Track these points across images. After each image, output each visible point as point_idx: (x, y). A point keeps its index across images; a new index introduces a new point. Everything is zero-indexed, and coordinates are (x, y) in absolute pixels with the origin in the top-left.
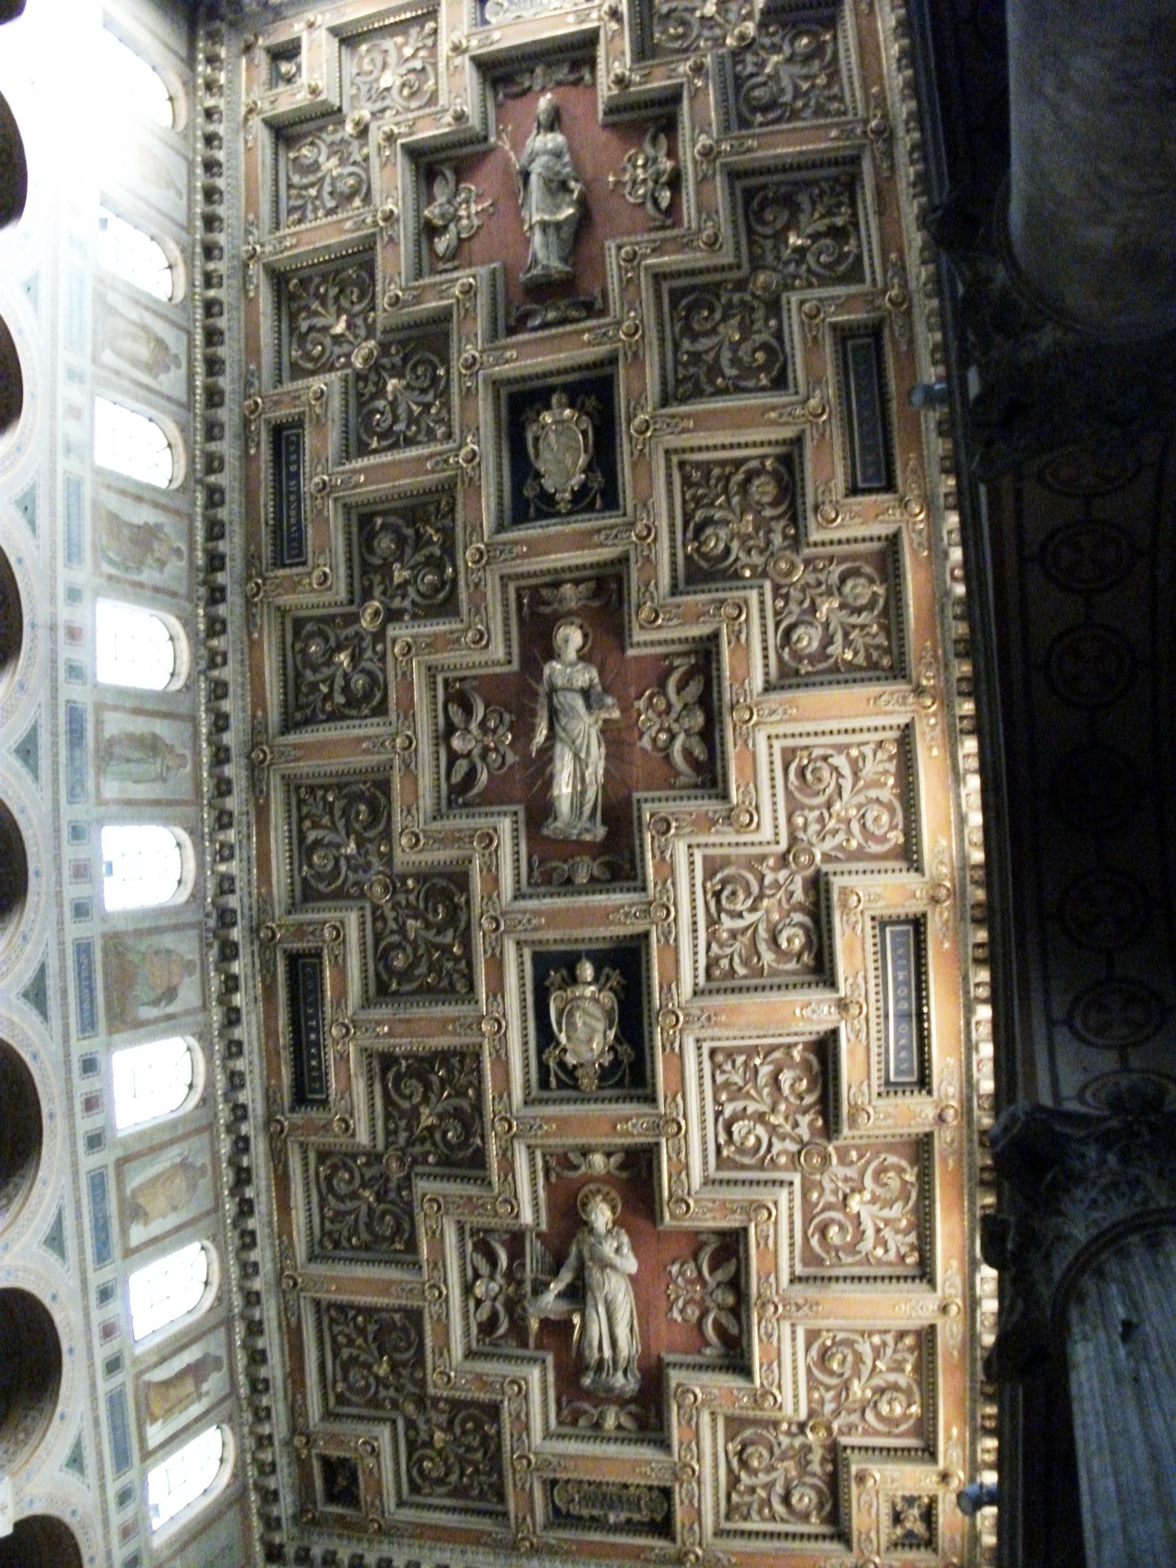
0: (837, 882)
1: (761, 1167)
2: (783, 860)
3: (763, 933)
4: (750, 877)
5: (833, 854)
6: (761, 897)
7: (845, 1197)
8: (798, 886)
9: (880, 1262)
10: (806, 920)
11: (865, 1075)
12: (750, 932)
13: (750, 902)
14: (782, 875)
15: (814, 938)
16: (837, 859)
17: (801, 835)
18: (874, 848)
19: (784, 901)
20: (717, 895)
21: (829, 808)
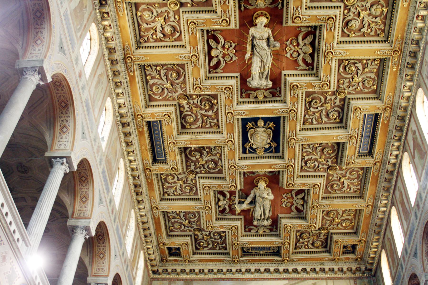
0: (353, 103)
1: (315, 171)
2: (334, 93)
3: (324, 113)
4: (322, 97)
5: (352, 92)
6: (325, 103)
7: (340, 178)
8: (338, 101)
9: (348, 193)
10: (340, 110)
11: (353, 154)
12: (320, 112)
13: (321, 104)
14: (333, 98)
15: (341, 115)
16: (353, 94)
17: (341, 86)
18: (366, 90)
19: (332, 104)
20: (310, 102)
21: (353, 79)
